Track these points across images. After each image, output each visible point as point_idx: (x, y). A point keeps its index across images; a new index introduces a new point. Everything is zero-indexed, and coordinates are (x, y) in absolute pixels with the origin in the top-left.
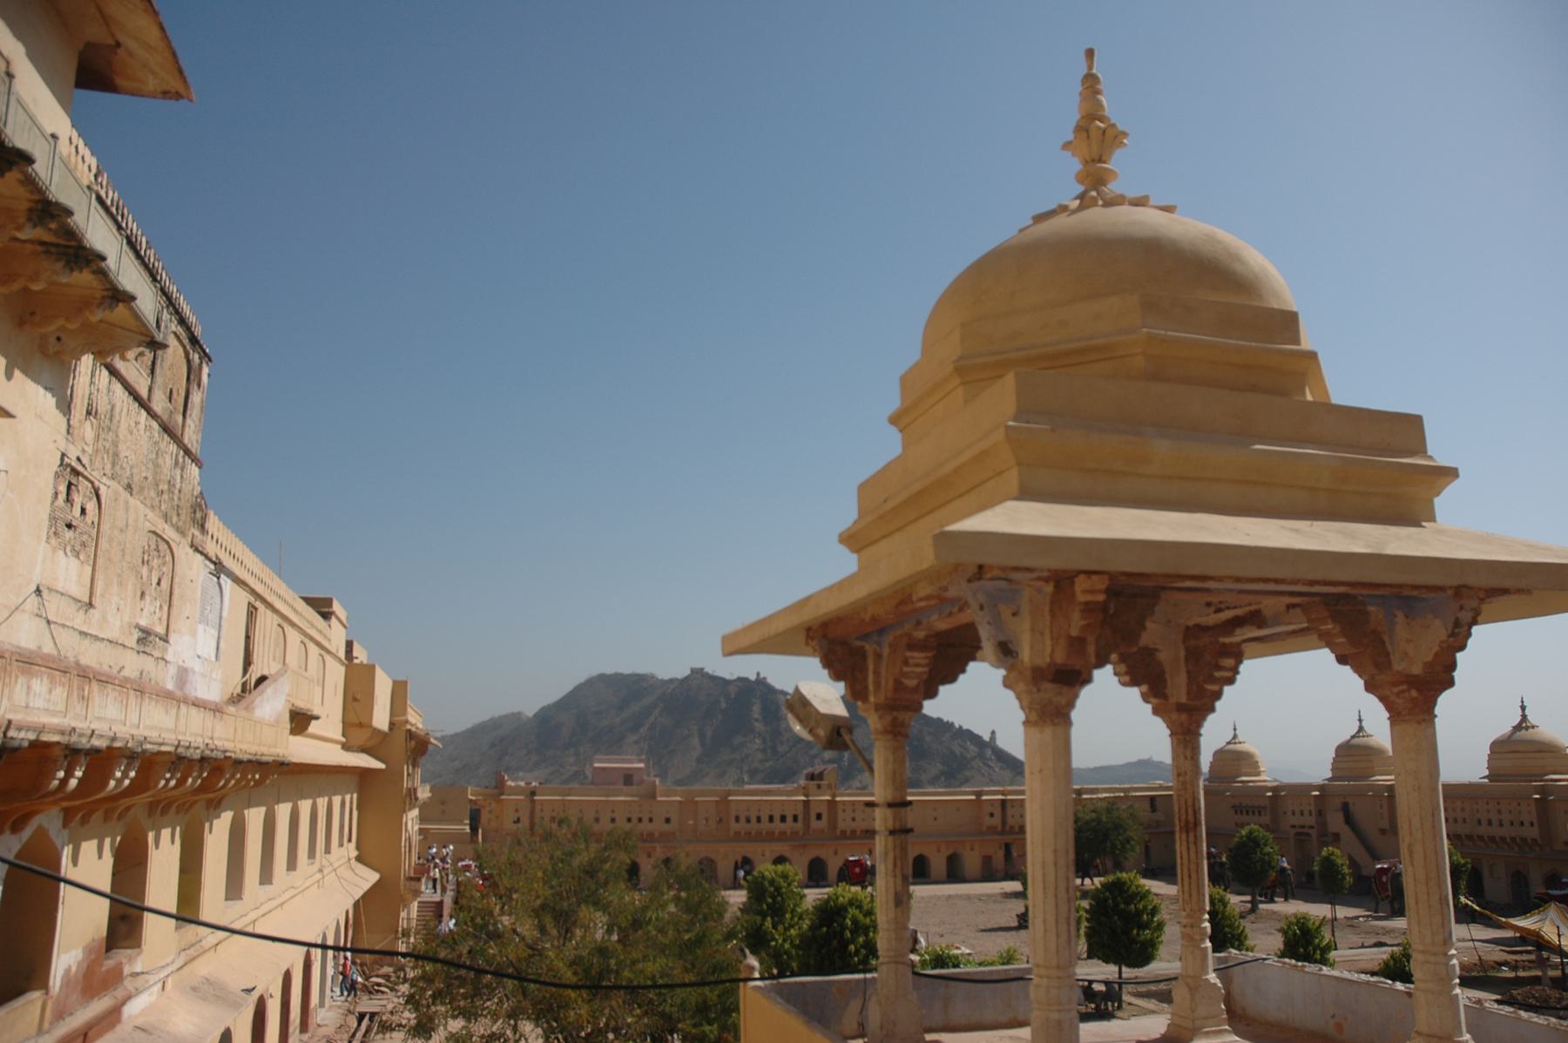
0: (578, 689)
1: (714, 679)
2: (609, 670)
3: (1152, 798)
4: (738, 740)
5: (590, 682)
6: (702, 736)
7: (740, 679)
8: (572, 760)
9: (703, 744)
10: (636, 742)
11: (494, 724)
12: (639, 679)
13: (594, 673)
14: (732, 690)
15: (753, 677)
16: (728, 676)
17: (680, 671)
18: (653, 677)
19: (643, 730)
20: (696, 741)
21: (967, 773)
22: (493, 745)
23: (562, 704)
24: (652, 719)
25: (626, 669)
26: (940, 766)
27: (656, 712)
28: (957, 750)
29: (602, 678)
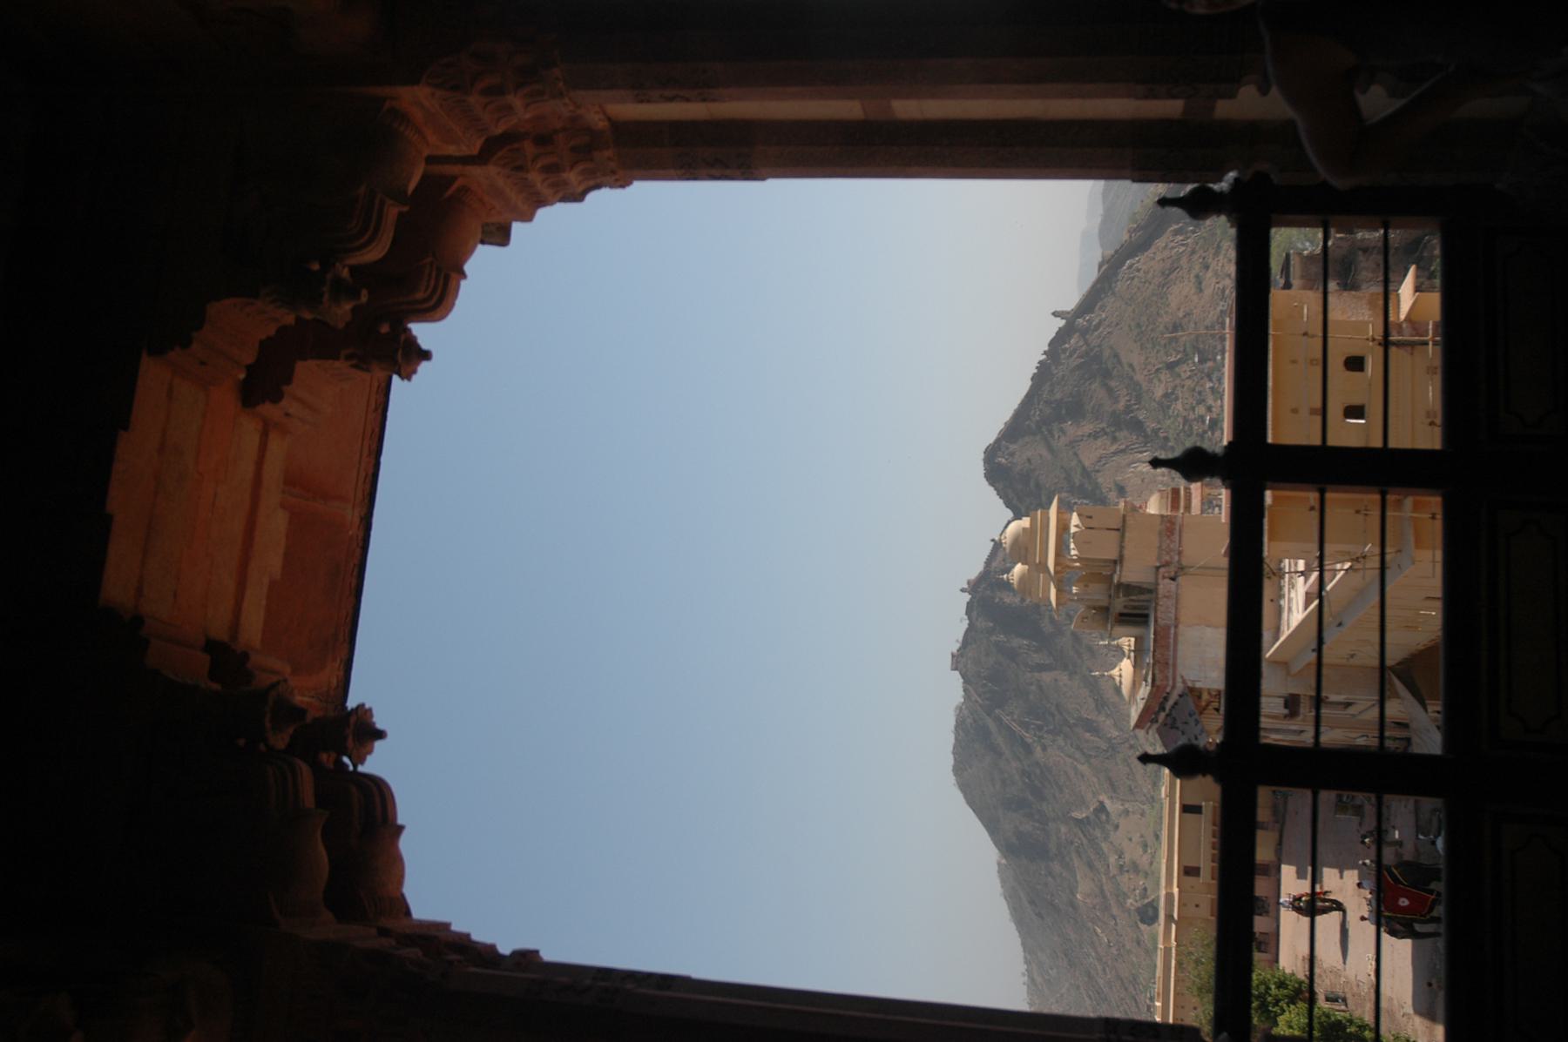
0: (971, 803)
1: (966, 642)
2: (950, 761)
3: (1186, 809)
4: (1047, 627)
5: (964, 787)
6: (1041, 668)
8: (1063, 829)
10: (1044, 748)
11: (1011, 896)
12: (960, 726)
13: (952, 779)
14: (982, 624)
15: (967, 597)
17: (956, 680)
18: (959, 709)
20: (1047, 677)
21: (1107, 353)
22: (1039, 915)
24: (1016, 727)
27: (1006, 719)
29: (958, 770)
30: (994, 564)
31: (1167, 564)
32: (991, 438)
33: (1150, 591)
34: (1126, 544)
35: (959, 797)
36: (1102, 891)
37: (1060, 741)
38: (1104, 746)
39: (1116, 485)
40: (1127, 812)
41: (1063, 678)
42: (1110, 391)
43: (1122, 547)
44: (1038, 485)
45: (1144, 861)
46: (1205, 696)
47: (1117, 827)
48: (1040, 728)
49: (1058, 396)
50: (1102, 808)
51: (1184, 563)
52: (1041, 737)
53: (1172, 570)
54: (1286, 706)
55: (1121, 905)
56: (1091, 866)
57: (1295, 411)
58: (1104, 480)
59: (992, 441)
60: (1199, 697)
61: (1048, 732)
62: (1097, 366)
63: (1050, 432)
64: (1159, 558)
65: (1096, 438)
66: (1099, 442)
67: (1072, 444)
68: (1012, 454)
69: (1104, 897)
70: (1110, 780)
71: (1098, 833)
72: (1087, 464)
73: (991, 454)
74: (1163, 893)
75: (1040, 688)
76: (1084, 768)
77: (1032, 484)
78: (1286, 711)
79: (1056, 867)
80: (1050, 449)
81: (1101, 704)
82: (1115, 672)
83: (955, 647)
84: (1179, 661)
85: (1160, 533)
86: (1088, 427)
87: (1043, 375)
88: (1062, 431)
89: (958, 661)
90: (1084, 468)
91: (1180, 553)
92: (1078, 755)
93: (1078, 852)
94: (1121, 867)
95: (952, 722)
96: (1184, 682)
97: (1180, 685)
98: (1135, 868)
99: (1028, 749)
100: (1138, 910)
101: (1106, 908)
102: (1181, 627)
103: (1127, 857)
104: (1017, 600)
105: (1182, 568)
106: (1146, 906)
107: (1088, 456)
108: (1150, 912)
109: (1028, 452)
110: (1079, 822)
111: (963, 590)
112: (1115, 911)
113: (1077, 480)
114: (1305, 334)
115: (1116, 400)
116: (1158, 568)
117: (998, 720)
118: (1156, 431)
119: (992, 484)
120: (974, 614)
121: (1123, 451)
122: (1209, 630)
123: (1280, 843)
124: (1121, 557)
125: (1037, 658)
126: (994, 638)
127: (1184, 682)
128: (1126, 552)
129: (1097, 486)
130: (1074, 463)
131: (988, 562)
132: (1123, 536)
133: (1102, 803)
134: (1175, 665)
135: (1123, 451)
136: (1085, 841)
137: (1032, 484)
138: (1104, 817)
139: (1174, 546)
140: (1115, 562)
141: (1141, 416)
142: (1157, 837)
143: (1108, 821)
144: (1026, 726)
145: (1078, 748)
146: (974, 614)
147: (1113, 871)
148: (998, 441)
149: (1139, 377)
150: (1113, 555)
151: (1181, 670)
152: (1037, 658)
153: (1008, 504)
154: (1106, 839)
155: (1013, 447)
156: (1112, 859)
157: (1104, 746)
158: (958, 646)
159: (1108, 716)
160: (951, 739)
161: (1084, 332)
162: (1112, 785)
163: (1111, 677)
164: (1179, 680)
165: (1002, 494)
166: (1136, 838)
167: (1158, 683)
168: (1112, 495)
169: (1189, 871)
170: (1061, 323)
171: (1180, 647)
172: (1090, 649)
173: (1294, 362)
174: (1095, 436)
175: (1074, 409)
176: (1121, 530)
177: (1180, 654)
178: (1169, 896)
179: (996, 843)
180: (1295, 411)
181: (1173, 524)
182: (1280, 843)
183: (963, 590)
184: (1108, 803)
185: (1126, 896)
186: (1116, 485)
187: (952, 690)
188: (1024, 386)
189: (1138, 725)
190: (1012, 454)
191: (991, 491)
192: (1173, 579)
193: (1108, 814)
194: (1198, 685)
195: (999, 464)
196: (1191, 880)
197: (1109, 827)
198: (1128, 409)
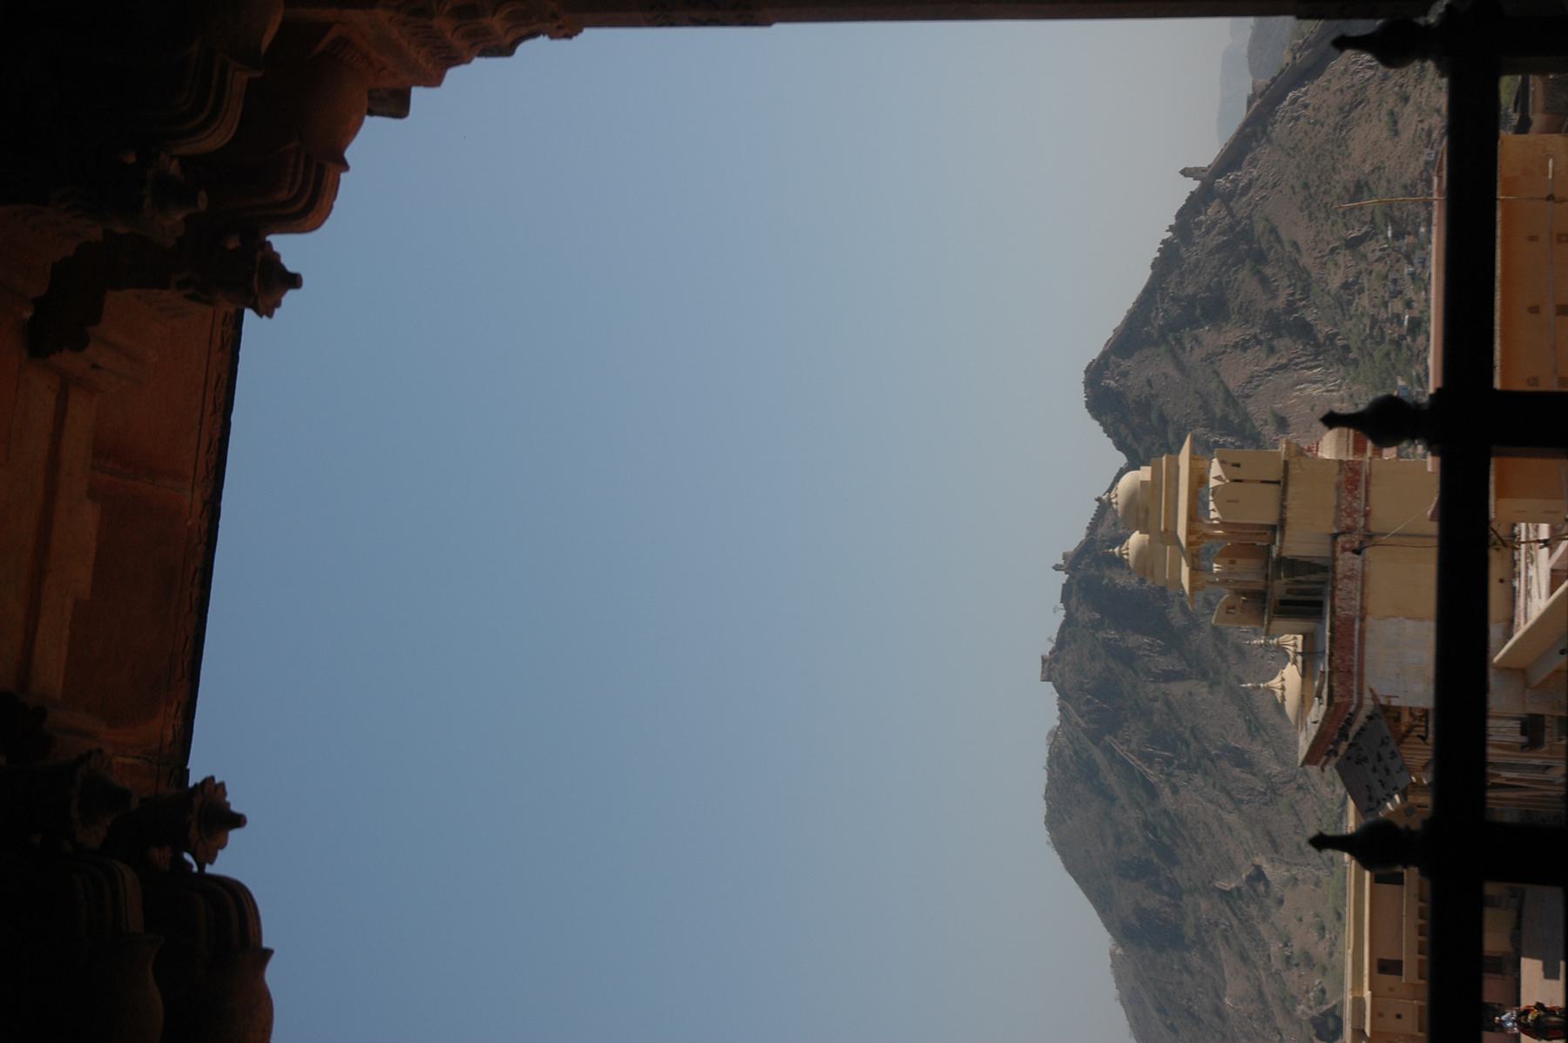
0: (1071, 868)
1: (1062, 642)
2: (1041, 809)
4: (1177, 618)
5: (1063, 846)
6: (1168, 676)
7: (1065, 598)
8: (1204, 905)
9: (1179, 676)
10: (1175, 790)
11: (1131, 1001)
12: (1056, 760)
13: (1044, 834)
14: (1086, 615)
15: (1063, 577)
16: (1060, 616)
18: (1054, 735)
19: (1153, 775)
20: (1177, 689)
21: (1259, 227)
23: (1102, 901)
24: (1133, 760)
25: (1038, 779)
26: (1244, 274)
27: (1121, 750)
28: (1215, 239)
30: (1101, 530)
31: (1349, 531)
32: (1095, 350)
33: (1324, 569)
34: (1290, 502)
35: (1056, 859)
36: (1261, 994)
37: (1198, 779)
38: (1261, 786)
39: (1275, 415)
40: (1295, 880)
41: (1202, 690)
42: (1264, 281)
43: (1283, 507)
44: (1163, 419)
45: (1320, 950)
46: (1406, 718)
47: (1281, 902)
48: (1169, 761)
49: (1190, 290)
50: (1258, 875)
51: (1373, 528)
52: (1170, 775)
53: (1356, 539)
54: (1523, 733)
55: (1289, 1013)
56: (1244, 958)
57: (1534, 310)
58: (1258, 410)
59: (1095, 356)
60: (1398, 719)
61: (1180, 767)
62: (1247, 247)
63: (1179, 341)
64: (1337, 521)
65: (1245, 349)
66: (1249, 355)
67: (1210, 358)
68: (1125, 374)
69: (1264, 1002)
70: (1269, 833)
71: (1253, 910)
72: (1232, 385)
73: (1095, 374)
74: (1349, 997)
75: (1167, 703)
76: (1232, 818)
77: (1154, 416)
78: (1524, 739)
79: (1195, 959)
80: (1181, 368)
81: (1255, 727)
82: (1275, 683)
83: (1048, 648)
84: (1367, 669)
85: (1338, 487)
86: (1233, 334)
87: (1168, 261)
88: (1196, 339)
89: (1050, 667)
90: (1227, 391)
91: (1367, 515)
92: (1223, 799)
93: (1226, 938)
94: (1288, 958)
95: (1043, 755)
96: (1375, 698)
97: (1368, 702)
98: (1308, 960)
99: (1152, 792)
100: (1313, 1020)
101: (1267, 1018)
102: (1369, 619)
103: (1296, 946)
104: (1134, 581)
105: (1370, 536)
106: (1325, 1015)
107: (1235, 373)
108: (1331, 1024)
109: (1152, 369)
110: (1225, 895)
111: (1057, 568)
112: (1280, 1021)
113: (1218, 410)
114: (1551, 198)
115: (1274, 297)
116: (1335, 537)
117: (1109, 750)
118: (1331, 338)
119: (1096, 417)
120: (1073, 601)
121: (1283, 367)
122: (1410, 624)
123: (1518, 926)
124: (1282, 522)
125: (1164, 663)
126: (1101, 635)
127: (1375, 698)
128: (1289, 515)
129: (1246, 417)
130: (1213, 385)
131: (1093, 527)
132: (1284, 491)
133: (1258, 868)
134: (1361, 675)
135: (1283, 367)
136: (1235, 922)
137: (1154, 416)
138: (1261, 888)
139: (1359, 505)
140: (1273, 528)
141: (1310, 316)
142: (1340, 916)
143: (1267, 894)
144: (1149, 759)
145: (1224, 789)
146: (1073, 601)
147: (1277, 964)
148: (1104, 355)
149: (1306, 260)
150: (1270, 518)
151: (1371, 681)
152: (1164, 663)
153: (1121, 446)
154: (1265, 919)
155: (1126, 364)
156: (1275, 947)
157: (1261, 786)
158: (1050, 646)
159: (1266, 743)
160: (1042, 778)
161: (1227, 198)
162: (1273, 841)
163: (1270, 691)
164: (1367, 694)
165: (1111, 431)
166: (1308, 917)
167: (1337, 700)
168: (1269, 431)
169: (1386, 967)
170: (1194, 185)
171: (1369, 649)
172: (1240, 651)
173: (1533, 239)
174: (1243, 346)
175: (1215, 309)
176: (1282, 483)
177: (1367, 658)
178: (1358, 1003)
179: (1109, 925)
180: (1534, 310)
181: (1357, 473)
182: (1518, 927)
183: (1057, 568)
184: (1267, 868)
185: (1295, 1000)
186: (1275, 415)
187: (1040, 710)
188: (1143, 275)
189: (1311, 758)
190: (1125, 374)
191: (1096, 428)
192: (1357, 552)
193: (1267, 884)
194: (1395, 702)
195: (1107, 388)
196: (1388, 980)
197: (1268, 902)
198: (1291, 307)
